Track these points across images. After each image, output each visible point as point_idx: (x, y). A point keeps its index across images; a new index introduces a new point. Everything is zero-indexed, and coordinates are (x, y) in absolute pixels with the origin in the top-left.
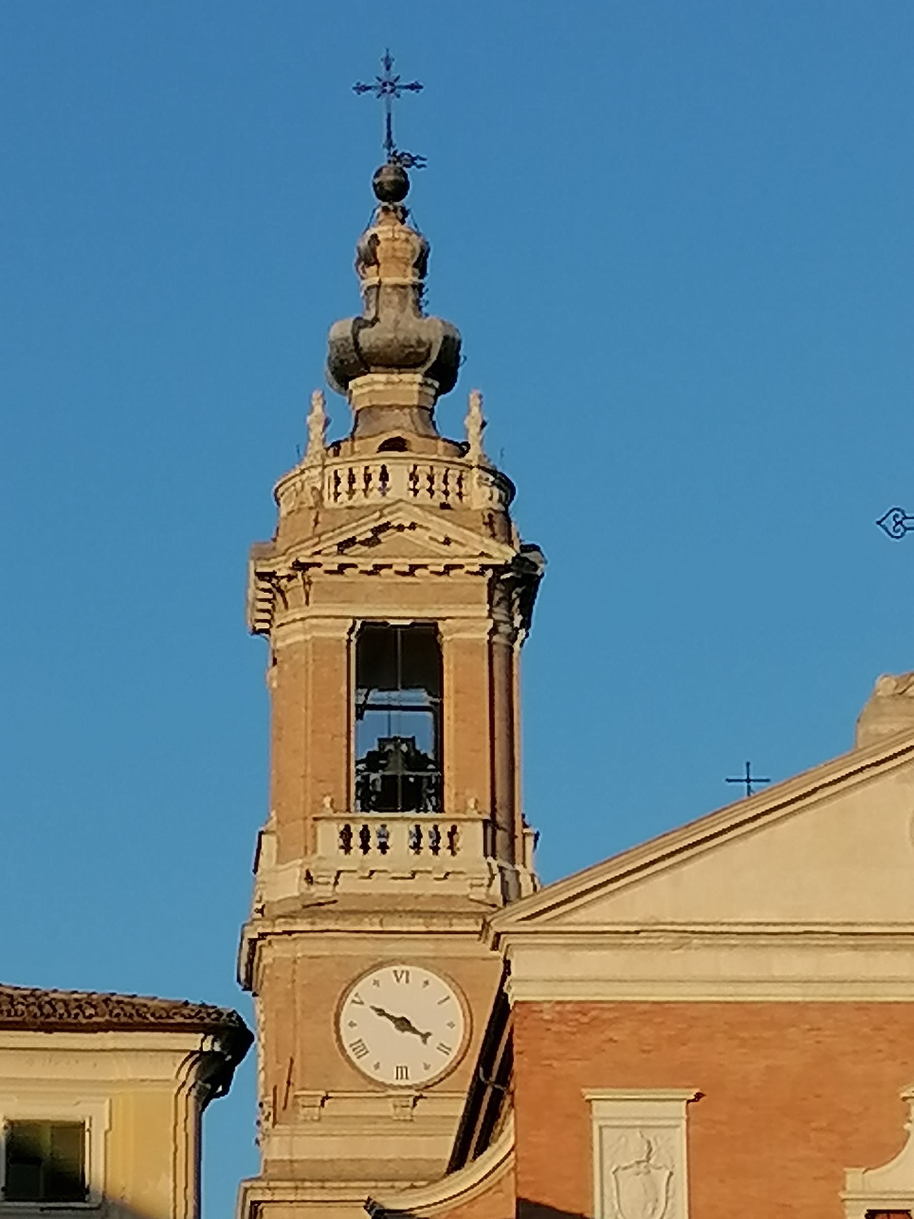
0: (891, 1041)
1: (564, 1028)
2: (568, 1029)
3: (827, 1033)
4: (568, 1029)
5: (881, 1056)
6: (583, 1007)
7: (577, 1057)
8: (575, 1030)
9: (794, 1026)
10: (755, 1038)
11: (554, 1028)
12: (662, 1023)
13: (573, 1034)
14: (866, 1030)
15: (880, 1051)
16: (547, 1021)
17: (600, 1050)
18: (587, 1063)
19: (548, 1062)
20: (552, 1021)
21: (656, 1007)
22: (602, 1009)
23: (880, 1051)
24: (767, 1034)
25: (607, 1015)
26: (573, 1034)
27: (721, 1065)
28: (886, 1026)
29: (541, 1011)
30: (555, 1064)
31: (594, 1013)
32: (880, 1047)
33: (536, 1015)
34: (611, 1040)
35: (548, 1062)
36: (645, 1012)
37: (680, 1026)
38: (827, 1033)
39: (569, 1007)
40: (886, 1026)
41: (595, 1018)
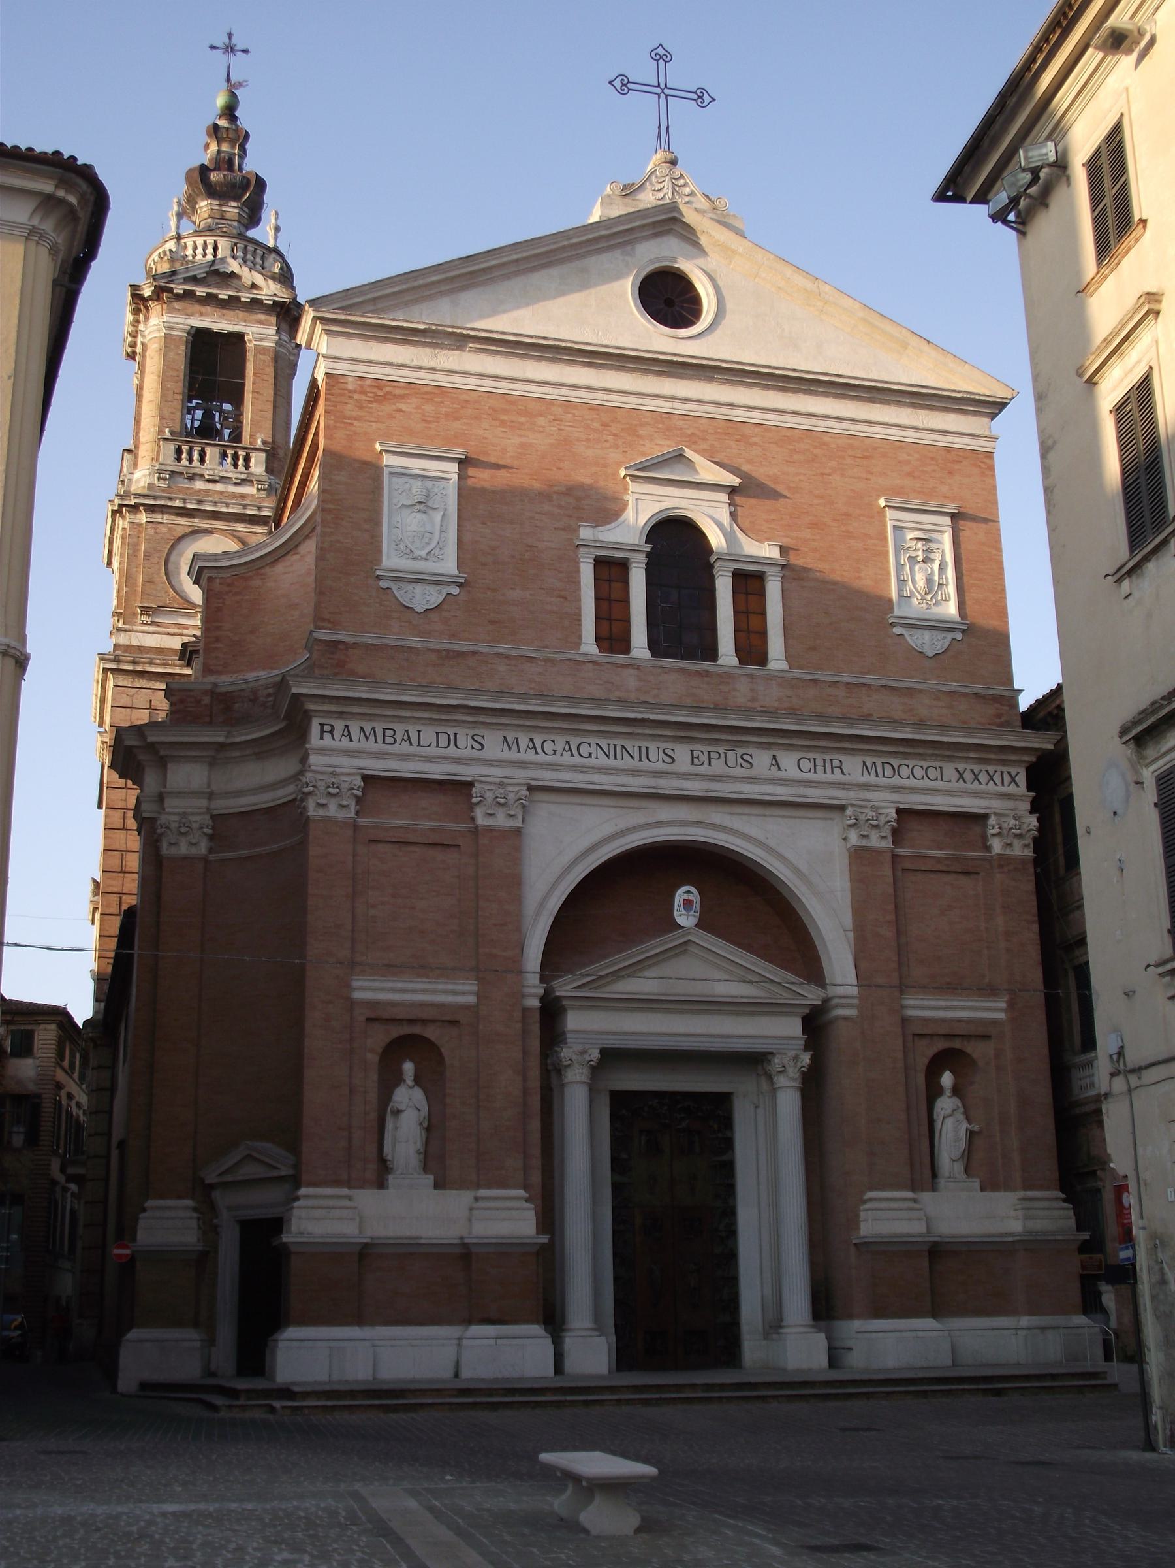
0: (615, 435)
1: (364, 397)
3: (567, 424)
4: (368, 399)
5: (608, 445)
6: (379, 383)
7: (373, 419)
8: (372, 399)
9: (541, 415)
10: (512, 422)
11: (356, 396)
12: (441, 402)
13: (370, 402)
14: (596, 425)
15: (606, 441)
16: (350, 391)
17: (391, 417)
18: (380, 425)
19: (349, 421)
20: (355, 391)
21: (436, 391)
22: (394, 387)
23: (606, 441)
24: (523, 420)
25: (398, 392)
26: (370, 402)
27: (486, 438)
28: (611, 424)
29: (346, 383)
30: (356, 423)
31: (388, 389)
32: (605, 437)
33: (342, 386)
34: (400, 410)
35: (349, 421)
36: (427, 393)
37: (455, 406)
38: (567, 424)
39: (368, 382)
40: (612, 424)
41: (389, 393)
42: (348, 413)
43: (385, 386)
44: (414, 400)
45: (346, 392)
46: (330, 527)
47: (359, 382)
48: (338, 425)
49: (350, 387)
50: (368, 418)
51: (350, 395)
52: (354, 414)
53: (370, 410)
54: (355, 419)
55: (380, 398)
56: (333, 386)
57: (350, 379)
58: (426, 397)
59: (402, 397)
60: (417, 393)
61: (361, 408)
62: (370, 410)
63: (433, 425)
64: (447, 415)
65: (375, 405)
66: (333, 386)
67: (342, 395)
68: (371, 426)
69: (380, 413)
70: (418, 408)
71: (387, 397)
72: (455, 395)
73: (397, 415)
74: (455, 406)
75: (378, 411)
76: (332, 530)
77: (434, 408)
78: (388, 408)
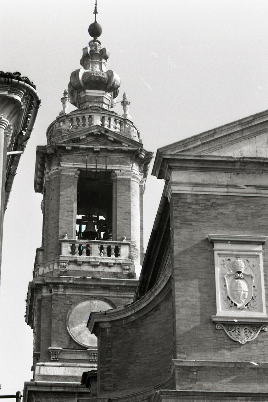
1: (198, 207)
2: (200, 208)
6: (207, 197)
8: (204, 208)
11: (193, 207)
13: (202, 210)
16: (189, 204)
20: (192, 204)
21: (244, 199)
22: (217, 199)
25: (219, 202)
26: (202, 210)
29: (187, 199)
30: (194, 223)
31: (213, 200)
33: (183, 200)
34: (222, 213)
39: (201, 197)
41: (214, 203)
42: (188, 218)
43: (211, 199)
44: (231, 207)
45: (186, 204)
46: (181, 292)
47: (194, 198)
48: (182, 225)
49: (189, 201)
50: (201, 220)
51: (189, 206)
52: (193, 218)
53: (203, 215)
54: (194, 221)
55: (208, 206)
56: (178, 201)
57: (189, 196)
58: (238, 203)
59: (223, 205)
60: (232, 202)
61: (197, 214)
62: (203, 215)
63: (244, 222)
64: (252, 214)
65: (205, 211)
66: (178, 201)
67: (184, 206)
68: (204, 225)
69: (209, 216)
70: (233, 211)
71: (214, 206)
72: (257, 201)
73: (220, 216)
74: (257, 208)
75: (208, 215)
76: (183, 293)
77: (244, 210)
78: (213, 213)
